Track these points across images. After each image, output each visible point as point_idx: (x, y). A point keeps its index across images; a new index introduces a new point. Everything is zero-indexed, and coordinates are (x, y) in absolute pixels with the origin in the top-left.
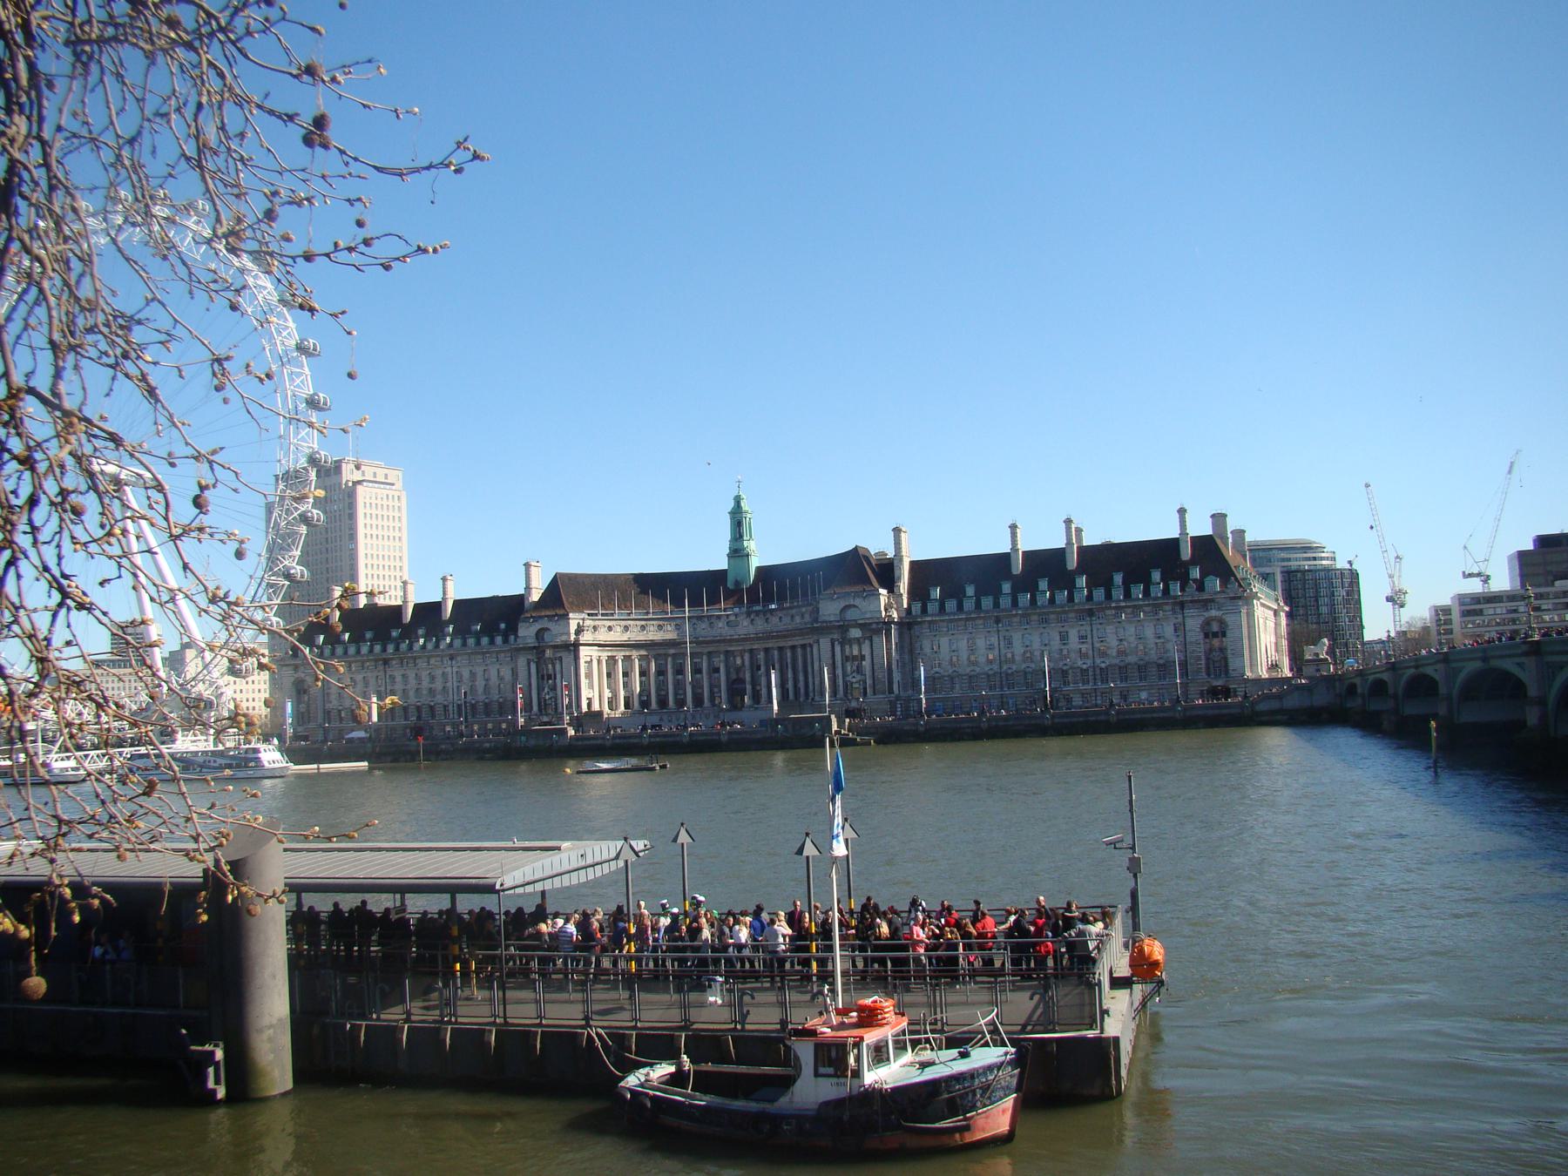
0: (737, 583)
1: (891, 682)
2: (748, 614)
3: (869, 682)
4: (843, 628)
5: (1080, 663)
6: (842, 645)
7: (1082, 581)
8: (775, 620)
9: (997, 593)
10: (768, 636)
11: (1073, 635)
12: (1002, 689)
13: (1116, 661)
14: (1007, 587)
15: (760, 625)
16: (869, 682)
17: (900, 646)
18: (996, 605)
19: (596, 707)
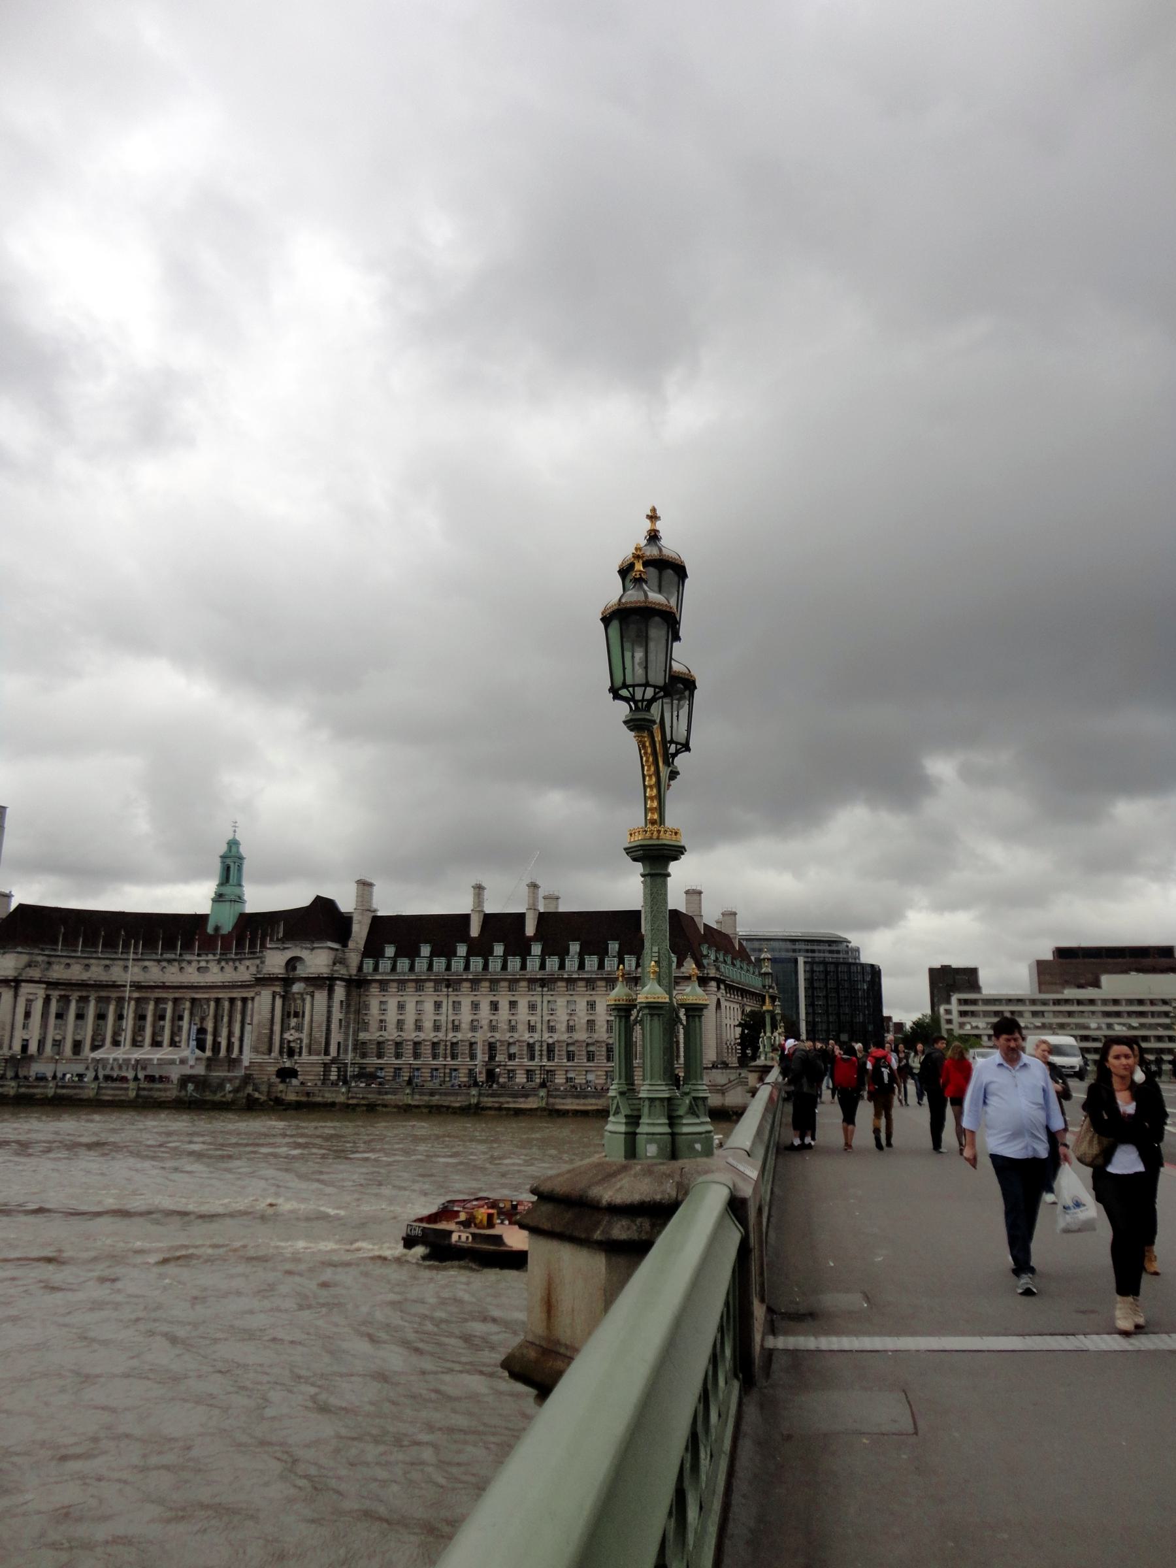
0: (217, 929)
1: (327, 1044)
2: (219, 961)
3: (305, 1041)
4: (287, 982)
5: (526, 1036)
6: (284, 998)
7: (536, 949)
8: (242, 968)
9: (450, 954)
10: (233, 986)
11: (523, 1005)
12: (445, 1058)
13: (565, 1037)
14: (462, 950)
15: (229, 975)
16: (305, 1041)
17: (346, 1005)
18: (448, 968)
19: (33, 1048)
